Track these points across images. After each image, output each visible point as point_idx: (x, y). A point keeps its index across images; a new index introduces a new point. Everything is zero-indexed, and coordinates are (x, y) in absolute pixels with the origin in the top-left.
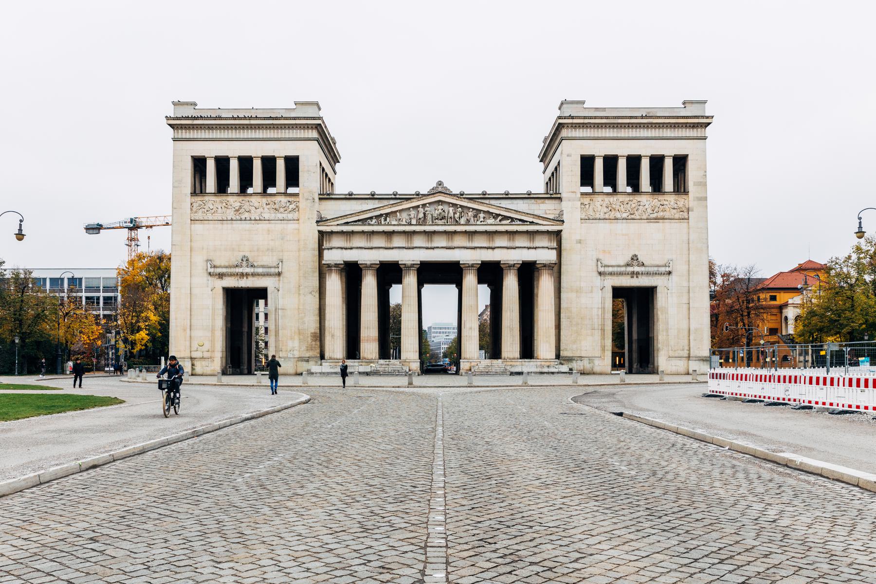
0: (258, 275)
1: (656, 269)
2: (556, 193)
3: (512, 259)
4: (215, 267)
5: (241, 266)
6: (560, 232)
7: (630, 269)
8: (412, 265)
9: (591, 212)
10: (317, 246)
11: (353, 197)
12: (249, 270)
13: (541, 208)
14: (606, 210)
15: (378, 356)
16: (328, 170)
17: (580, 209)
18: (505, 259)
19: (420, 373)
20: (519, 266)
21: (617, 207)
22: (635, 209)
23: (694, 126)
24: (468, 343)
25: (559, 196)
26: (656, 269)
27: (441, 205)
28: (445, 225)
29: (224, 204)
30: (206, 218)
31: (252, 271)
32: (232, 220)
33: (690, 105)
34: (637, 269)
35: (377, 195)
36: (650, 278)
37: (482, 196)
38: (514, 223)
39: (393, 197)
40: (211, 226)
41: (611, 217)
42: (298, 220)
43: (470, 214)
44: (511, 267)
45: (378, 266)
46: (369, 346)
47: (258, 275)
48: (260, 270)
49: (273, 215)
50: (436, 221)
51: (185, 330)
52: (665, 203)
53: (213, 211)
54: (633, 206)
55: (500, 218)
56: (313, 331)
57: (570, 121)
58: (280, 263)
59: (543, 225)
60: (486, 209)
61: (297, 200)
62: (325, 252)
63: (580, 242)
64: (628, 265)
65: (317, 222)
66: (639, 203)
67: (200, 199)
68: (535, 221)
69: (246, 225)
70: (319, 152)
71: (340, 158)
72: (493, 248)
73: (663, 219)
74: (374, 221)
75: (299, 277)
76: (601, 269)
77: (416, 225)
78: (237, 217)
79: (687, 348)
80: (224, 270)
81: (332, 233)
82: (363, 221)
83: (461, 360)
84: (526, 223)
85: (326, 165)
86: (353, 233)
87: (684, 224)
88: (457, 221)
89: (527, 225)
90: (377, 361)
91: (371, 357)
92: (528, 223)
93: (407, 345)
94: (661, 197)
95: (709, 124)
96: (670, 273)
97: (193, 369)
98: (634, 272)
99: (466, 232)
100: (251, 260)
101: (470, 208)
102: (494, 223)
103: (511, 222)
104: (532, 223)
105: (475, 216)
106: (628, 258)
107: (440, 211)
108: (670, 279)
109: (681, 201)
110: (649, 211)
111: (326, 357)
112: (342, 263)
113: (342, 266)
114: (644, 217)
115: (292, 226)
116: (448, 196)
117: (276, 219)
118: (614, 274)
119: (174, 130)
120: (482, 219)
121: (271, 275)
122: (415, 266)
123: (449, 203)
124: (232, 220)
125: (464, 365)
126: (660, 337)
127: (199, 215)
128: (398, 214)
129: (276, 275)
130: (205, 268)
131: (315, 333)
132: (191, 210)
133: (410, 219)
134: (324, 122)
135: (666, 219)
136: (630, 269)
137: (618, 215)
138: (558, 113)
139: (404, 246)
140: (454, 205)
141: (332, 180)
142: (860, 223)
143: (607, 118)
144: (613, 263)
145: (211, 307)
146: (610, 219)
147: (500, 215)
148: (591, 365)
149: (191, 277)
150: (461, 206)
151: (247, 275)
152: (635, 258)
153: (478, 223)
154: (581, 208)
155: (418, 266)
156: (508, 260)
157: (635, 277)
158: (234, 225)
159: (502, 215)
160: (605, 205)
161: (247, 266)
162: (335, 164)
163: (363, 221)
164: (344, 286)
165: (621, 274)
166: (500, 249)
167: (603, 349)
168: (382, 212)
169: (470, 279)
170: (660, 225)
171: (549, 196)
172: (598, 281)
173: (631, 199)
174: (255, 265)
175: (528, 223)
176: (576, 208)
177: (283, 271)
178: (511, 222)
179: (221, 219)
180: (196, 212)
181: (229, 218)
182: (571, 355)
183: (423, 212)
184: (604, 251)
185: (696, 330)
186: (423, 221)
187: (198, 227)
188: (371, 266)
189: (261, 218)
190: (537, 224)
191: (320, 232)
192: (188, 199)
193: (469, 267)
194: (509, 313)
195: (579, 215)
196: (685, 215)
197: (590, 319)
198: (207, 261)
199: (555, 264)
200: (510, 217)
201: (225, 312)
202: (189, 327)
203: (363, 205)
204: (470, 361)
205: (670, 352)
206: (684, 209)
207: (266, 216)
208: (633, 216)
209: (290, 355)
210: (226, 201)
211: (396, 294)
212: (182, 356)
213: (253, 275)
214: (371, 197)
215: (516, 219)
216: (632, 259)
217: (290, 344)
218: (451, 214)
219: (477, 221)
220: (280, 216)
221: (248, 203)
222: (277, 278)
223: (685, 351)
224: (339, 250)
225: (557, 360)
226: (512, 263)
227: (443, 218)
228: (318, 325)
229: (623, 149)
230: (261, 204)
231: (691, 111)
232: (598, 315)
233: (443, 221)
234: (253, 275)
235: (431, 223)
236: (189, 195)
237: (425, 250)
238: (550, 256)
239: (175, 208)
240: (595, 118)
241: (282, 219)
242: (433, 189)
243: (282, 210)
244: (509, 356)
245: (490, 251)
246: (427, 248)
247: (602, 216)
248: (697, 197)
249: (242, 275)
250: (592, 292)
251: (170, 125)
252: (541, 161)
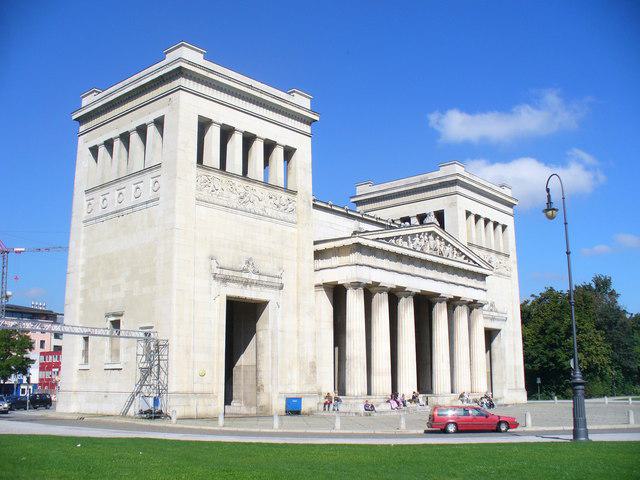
12: (255, 277)
34: (495, 314)
43: (448, 248)
48: (265, 279)
69: (251, 220)
82: (387, 239)
127: (205, 194)
130: (208, 266)
140: (441, 238)
147: (463, 254)
187: (202, 210)
207: (269, 212)
220: (282, 215)
236: (195, 164)
243: (283, 208)
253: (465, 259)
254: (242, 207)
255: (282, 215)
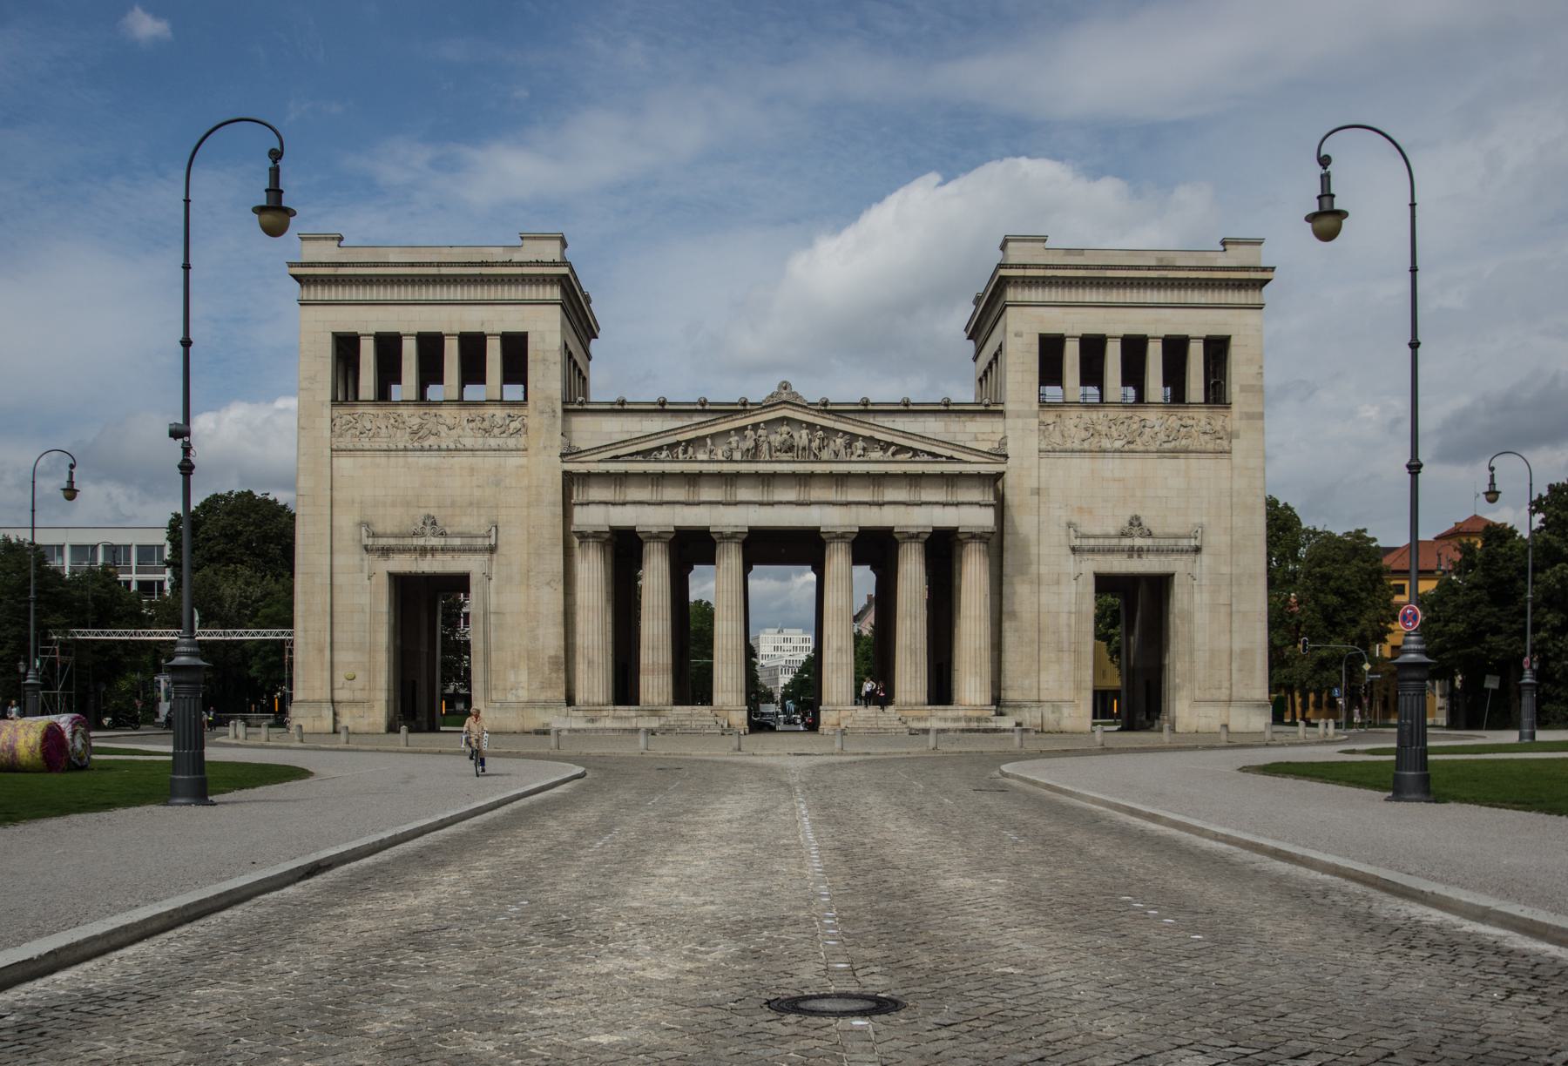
0: (453, 550)
1: (1172, 542)
2: (996, 404)
3: (915, 523)
4: (374, 535)
5: (423, 535)
6: (999, 476)
7: (1127, 542)
8: (733, 536)
9: (1057, 438)
10: (560, 497)
11: (626, 407)
13: (967, 430)
14: (1084, 434)
15: (671, 700)
16: (579, 356)
17: (1037, 432)
18: (902, 523)
19: (747, 731)
20: (927, 536)
21: (1104, 430)
22: (1136, 433)
23: (1240, 285)
24: (835, 676)
25: (1000, 408)
26: (1172, 542)
27: (787, 425)
28: (794, 462)
29: (392, 421)
30: (359, 446)
31: (443, 543)
32: (406, 450)
33: (1234, 246)
34: (1138, 542)
35: (671, 404)
36: (1162, 558)
37: (862, 408)
38: (917, 459)
39: (699, 407)
40: (366, 460)
41: (1093, 448)
42: (526, 450)
43: (839, 441)
44: (913, 537)
45: (672, 536)
46: (655, 682)
47: (453, 550)
48: (457, 542)
49: (480, 441)
50: (778, 453)
51: (321, 650)
52: (1190, 422)
53: (371, 434)
54: (1135, 427)
55: (893, 449)
56: (552, 653)
57: (1020, 272)
58: (494, 529)
59: (970, 462)
60: (867, 433)
61: (525, 413)
62: (577, 511)
63: (1038, 492)
64: (1123, 535)
65: (562, 455)
66: (1143, 423)
67: (348, 412)
68: (957, 455)
69: (432, 460)
70: (563, 325)
71: (598, 329)
72: (881, 504)
73: (1187, 451)
74: (664, 454)
75: (529, 554)
76: (1077, 542)
77: (741, 461)
78: (416, 444)
79: (1226, 684)
80: (392, 542)
81: (589, 475)
82: (646, 454)
83: (821, 708)
84: (939, 459)
85: (574, 347)
86: (626, 474)
87: (1223, 463)
88: (815, 454)
89: (942, 462)
90: (669, 708)
91: (661, 700)
92: (944, 459)
93: (725, 679)
94: (1181, 413)
95: (1267, 281)
96: (1197, 550)
97: (335, 721)
98: (1133, 547)
99: (831, 475)
100: (440, 523)
101: (839, 431)
102: (881, 459)
103: (913, 456)
104: (950, 459)
105: (849, 445)
106: (1122, 522)
107: (785, 436)
108: (1198, 562)
109: (1219, 419)
110: (1162, 436)
111: (577, 701)
112: (608, 530)
113: (607, 536)
114: (1153, 448)
115: (514, 461)
116: (800, 409)
117: (487, 447)
118: (1099, 551)
119: (302, 286)
120: (861, 452)
121: (476, 550)
122: (738, 536)
123: (801, 422)
124: (406, 450)
125: (827, 717)
126: (1178, 666)
127: (345, 442)
128: (709, 441)
129: (486, 550)
130: (357, 537)
131: (556, 657)
132: (332, 431)
133: (731, 450)
134: (572, 270)
135: (1192, 452)
136: (1127, 542)
137: (1106, 444)
138: (998, 257)
139: (719, 499)
141: (584, 373)
142: (1492, 477)
143: (1086, 267)
144: (1097, 531)
145: (367, 610)
146: (1091, 451)
147: (892, 444)
148: (1057, 715)
149: (332, 553)
150: (823, 428)
151: (433, 550)
152: (1136, 523)
153: (854, 458)
154: (1039, 430)
155: (745, 536)
156: (907, 527)
157: (1135, 556)
158: (410, 460)
159: (896, 445)
160: (1082, 426)
161: (434, 535)
162: (589, 341)
163: (646, 454)
164: (610, 571)
165: (1111, 551)
166: (893, 506)
167: (1078, 687)
168: (680, 437)
169: (838, 560)
170: (1181, 463)
171: (983, 408)
172: (1070, 564)
173: (1130, 414)
174: (448, 531)
175: (944, 459)
176: (1031, 431)
177: (499, 543)
178: (913, 456)
179: (385, 448)
180: (341, 435)
181: (401, 446)
182: (1020, 698)
183: (754, 437)
184: (1080, 509)
185: (1243, 652)
186: (753, 454)
187: (344, 463)
188: (657, 537)
189: (459, 446)
190: (960, 461)
191: (566, 474)
192: (327, 411)
193: (837, 537)
194: (908, 623)
195: (1034, 442)
196: (1225, 444)
197: (1054, 633)
198: (361, 524)
199: (993, 533)
200: (911, 449)
201: (392, 618)
202: (328, 645)
203: (644, 423)
204: (839, 708)
205: (1197, 692)
206: (1221, 435)
208: (1132, 446)
209: (511, 698)
210: (395, 416)
211: (706, 585)
212: (317, 697)
213: (444, 550)
214: (659, 407)
215: (922, 451)
216: (1131, 524)
217: (511, 677)
218: (805, 441)
219: (852, 454)
220: (493, 443)
221: (434, 420)
222: (487, 556)
223: (1224, 690)
224: (602, 508)
225: (994, 707)
226: (914, 531)
227: (790, 449)
228: (563, 643)
229: (1115, 323)
230: (458, 420)
231: (1236, 256)
232: (1069, 626)
233: (790, 454)
234: (444, 550)
235: (768, 458)
236: (330, 406)
237: (757, 508)
238: (983, 519)
239: (303, 428)
240: (1065, 267)
241: (497, 447)
242: (772, 396)
243: (496, 431)
244: (908, 700)
245: (875, 509)
246: (761, 504)
247: (1077, 446)
248: (1246, 413)
249: (424, 551)
250: (1058, 583)
251: (295, 277)
252: (969, 338)
253: (893, 454)
254: (420, 443)
255: (493, 443)
